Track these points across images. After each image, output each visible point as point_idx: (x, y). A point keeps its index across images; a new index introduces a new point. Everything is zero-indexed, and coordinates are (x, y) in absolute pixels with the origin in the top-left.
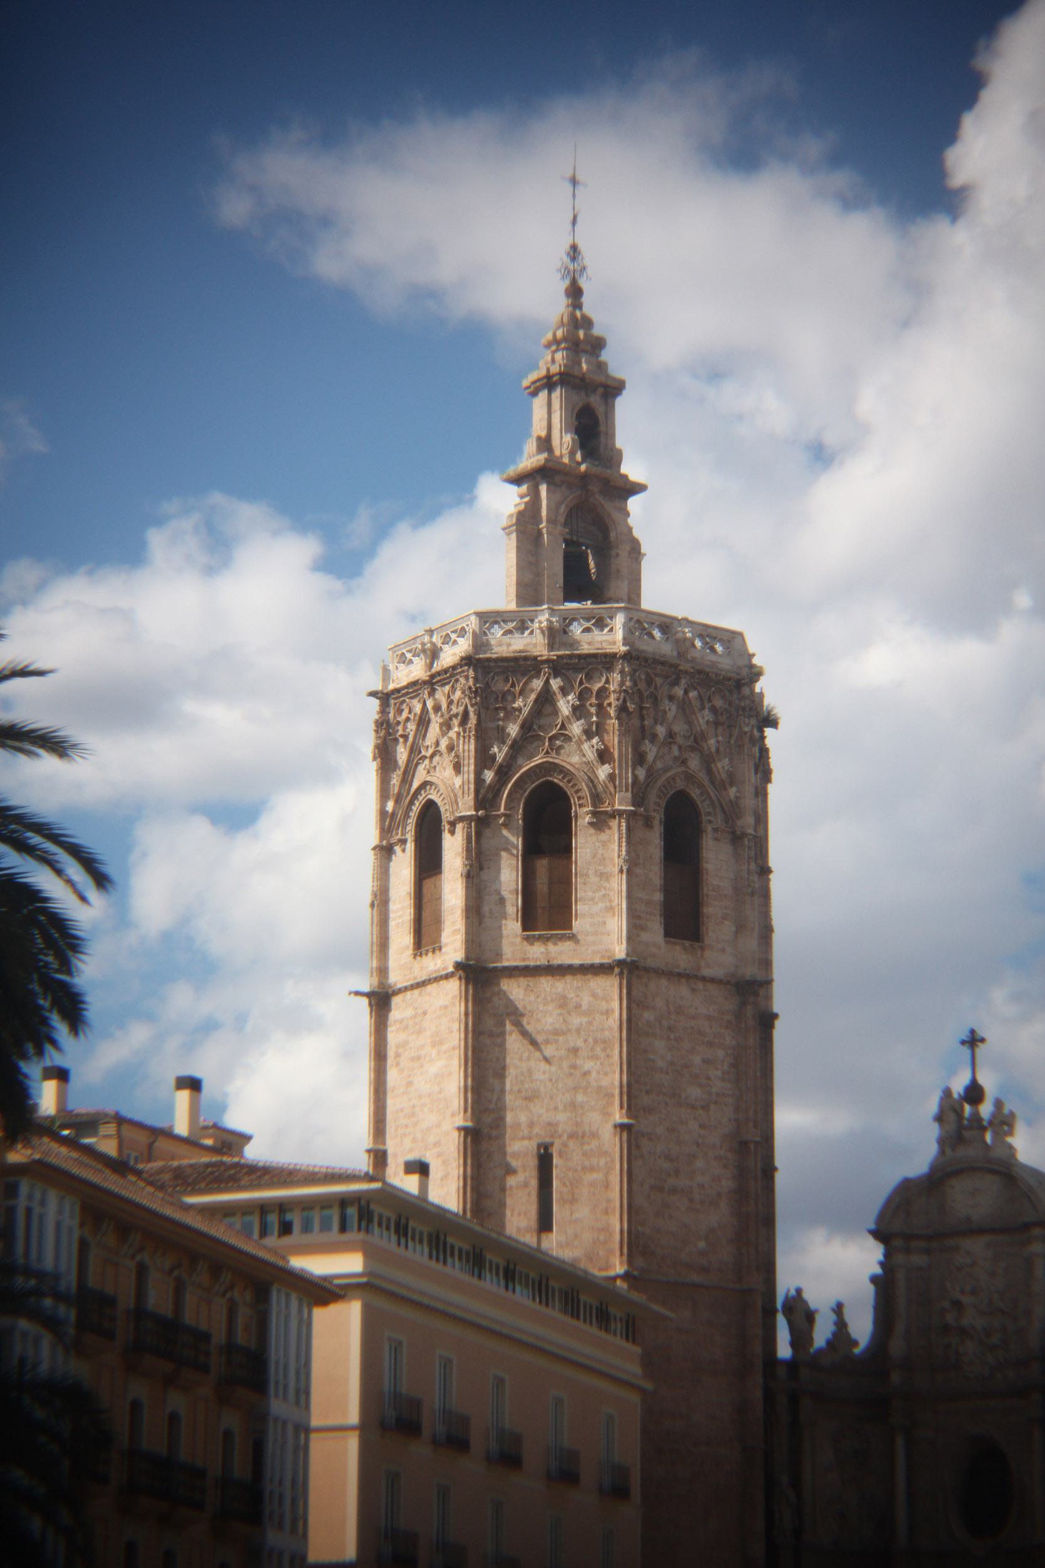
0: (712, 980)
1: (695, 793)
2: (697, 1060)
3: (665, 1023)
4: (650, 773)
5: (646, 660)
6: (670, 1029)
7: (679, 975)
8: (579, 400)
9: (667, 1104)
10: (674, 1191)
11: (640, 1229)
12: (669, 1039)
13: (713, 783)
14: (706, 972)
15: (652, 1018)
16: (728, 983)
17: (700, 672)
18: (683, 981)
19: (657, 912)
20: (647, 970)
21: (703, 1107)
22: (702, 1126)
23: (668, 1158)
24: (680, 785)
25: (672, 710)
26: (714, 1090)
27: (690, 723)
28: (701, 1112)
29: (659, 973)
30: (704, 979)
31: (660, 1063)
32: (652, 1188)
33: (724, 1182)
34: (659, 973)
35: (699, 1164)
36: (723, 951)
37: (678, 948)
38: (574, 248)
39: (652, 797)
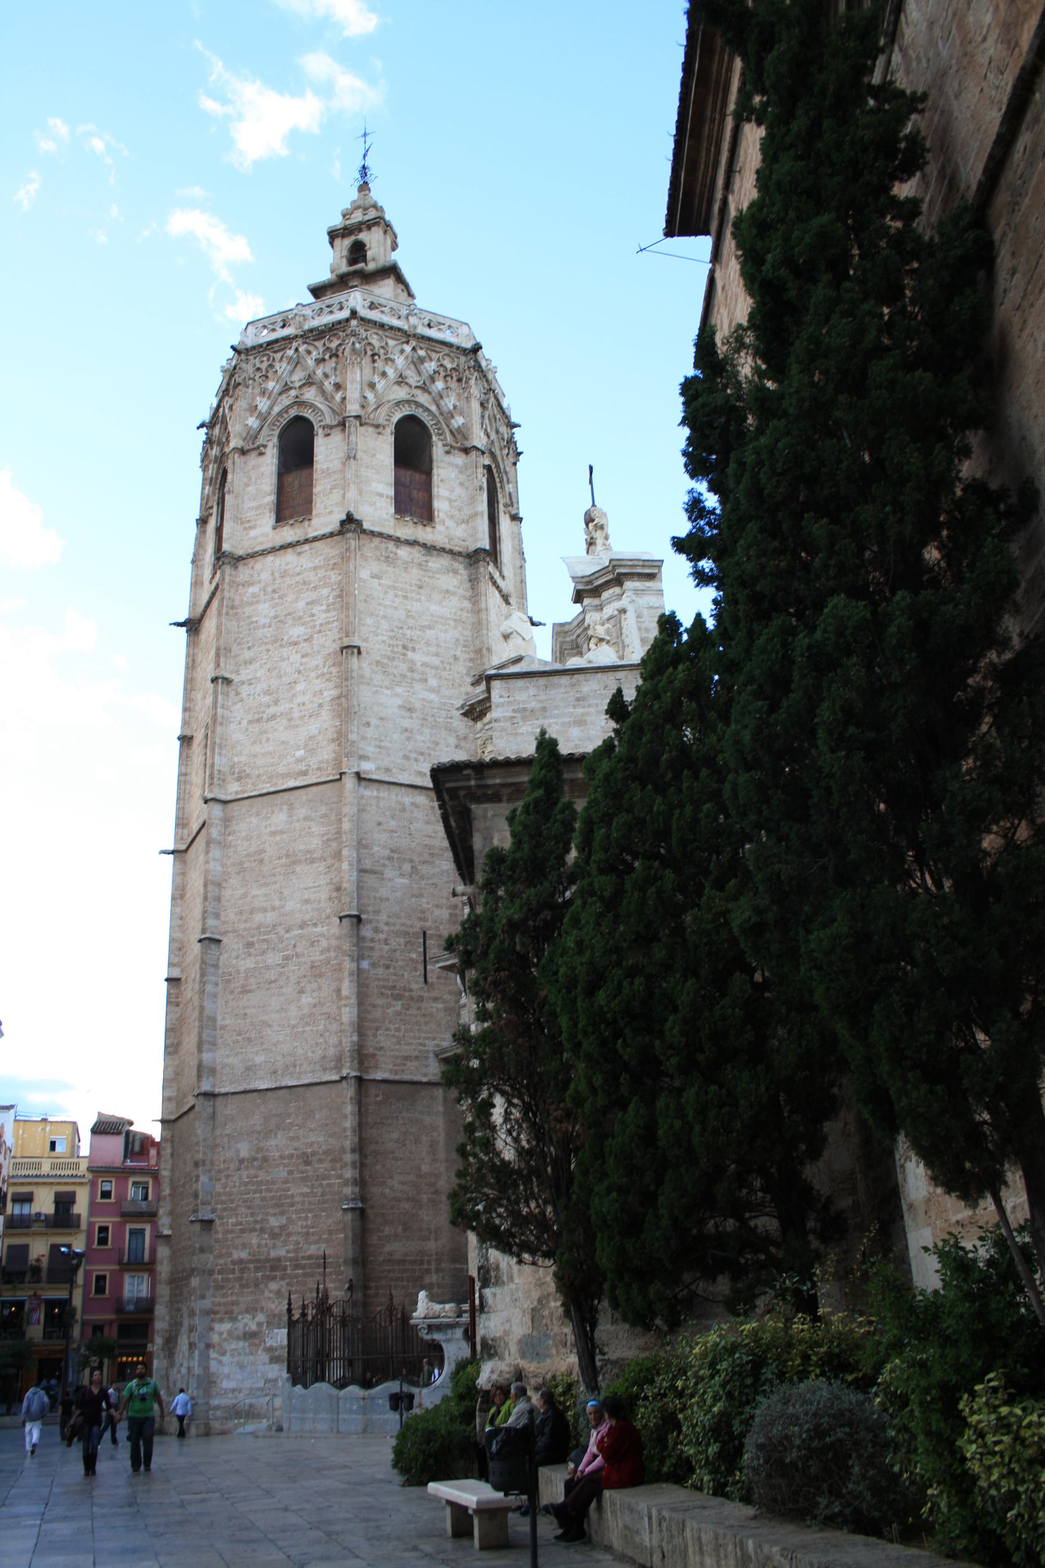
0: (315, 539)
1: (307, 414)
2: (301, 605)
3: (270, 589)
4: (263, 418)
5: (261, 346)
6: (274, 591)
7: (283, 547)
8: (348, 242)
9: (268, 650)
10: (273, 717)
11: (236, 759)
12: (273, 599)
13: (326, 399)
14: (311, 534)
15: (256, 590)
16: (332, 535)
17: (311, 331)
18: (290, 550)
19: (267, 511)
20: (253, 556)
21: (305, 640)
22: (303, 656)
23: (268, 692)
24: (293, 412)
25: (282, 367)
26: (318, 623)
27: (305, 369)
28: (304, 644)
29: (264, 553)
30: (307, 541)
31: (263, 621)
32: (250, 722)
33: (326, 693)
34: (264, 553)
35: (300, 687)
36: (331, 513)
37: (285, 528)
38: (364, 167)
39: (265, 431)
